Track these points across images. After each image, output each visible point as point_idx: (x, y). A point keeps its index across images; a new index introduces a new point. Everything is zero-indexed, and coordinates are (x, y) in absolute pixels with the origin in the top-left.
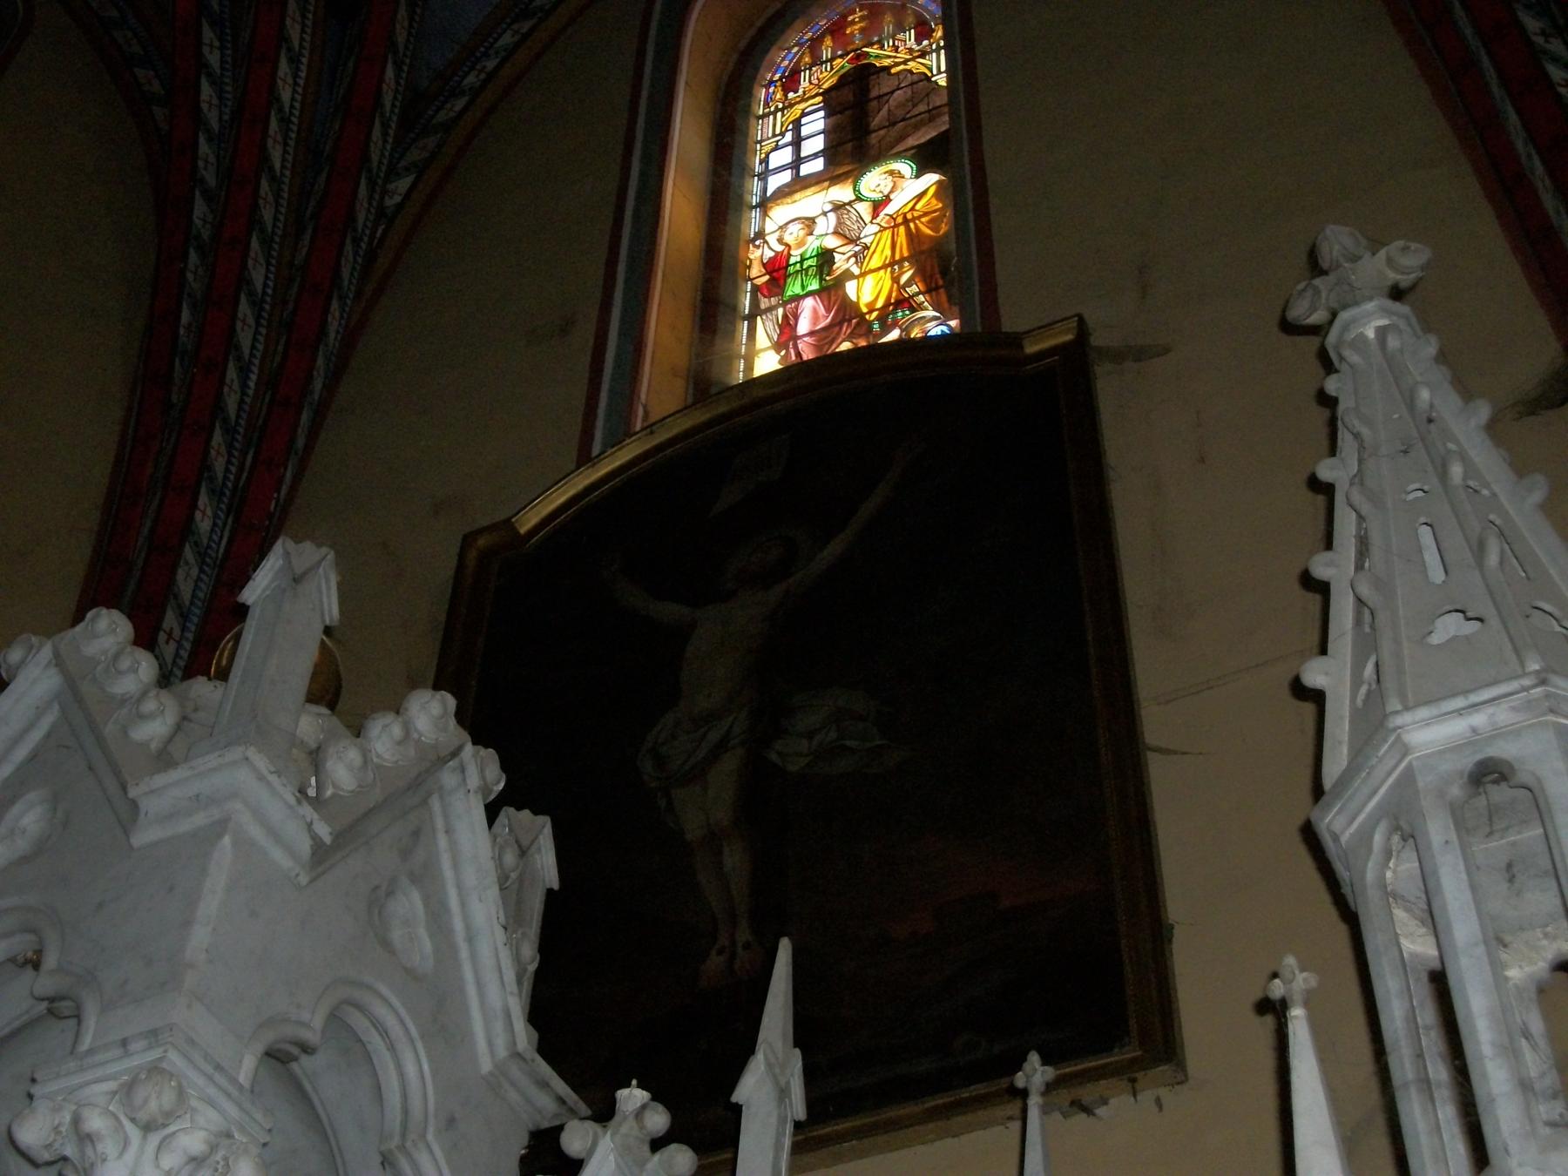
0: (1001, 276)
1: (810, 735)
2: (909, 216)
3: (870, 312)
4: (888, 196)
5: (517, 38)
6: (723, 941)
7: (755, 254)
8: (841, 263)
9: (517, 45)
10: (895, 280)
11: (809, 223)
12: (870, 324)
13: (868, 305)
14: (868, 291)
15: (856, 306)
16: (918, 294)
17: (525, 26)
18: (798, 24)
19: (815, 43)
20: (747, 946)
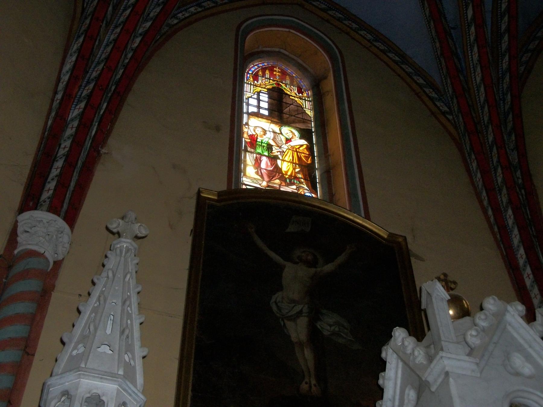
0: (369, 205)
1: (331, 326)
2: (298, 150)
3: (286, 175)
4: (291, 139)
5: (195, 11)
6: (307, 380)
7: (245, 130)
8: (275, 151)
9: (195, 14)
10: (294, 169)
11: (265, 132)
12: (286, 179)
13: (285, 172)
14: (286, 167)
15: (281, 169)
16: (302, 178)
17: (200, 9)
18: (259, 60)
19: (264, 70)
20: (315, 385)
